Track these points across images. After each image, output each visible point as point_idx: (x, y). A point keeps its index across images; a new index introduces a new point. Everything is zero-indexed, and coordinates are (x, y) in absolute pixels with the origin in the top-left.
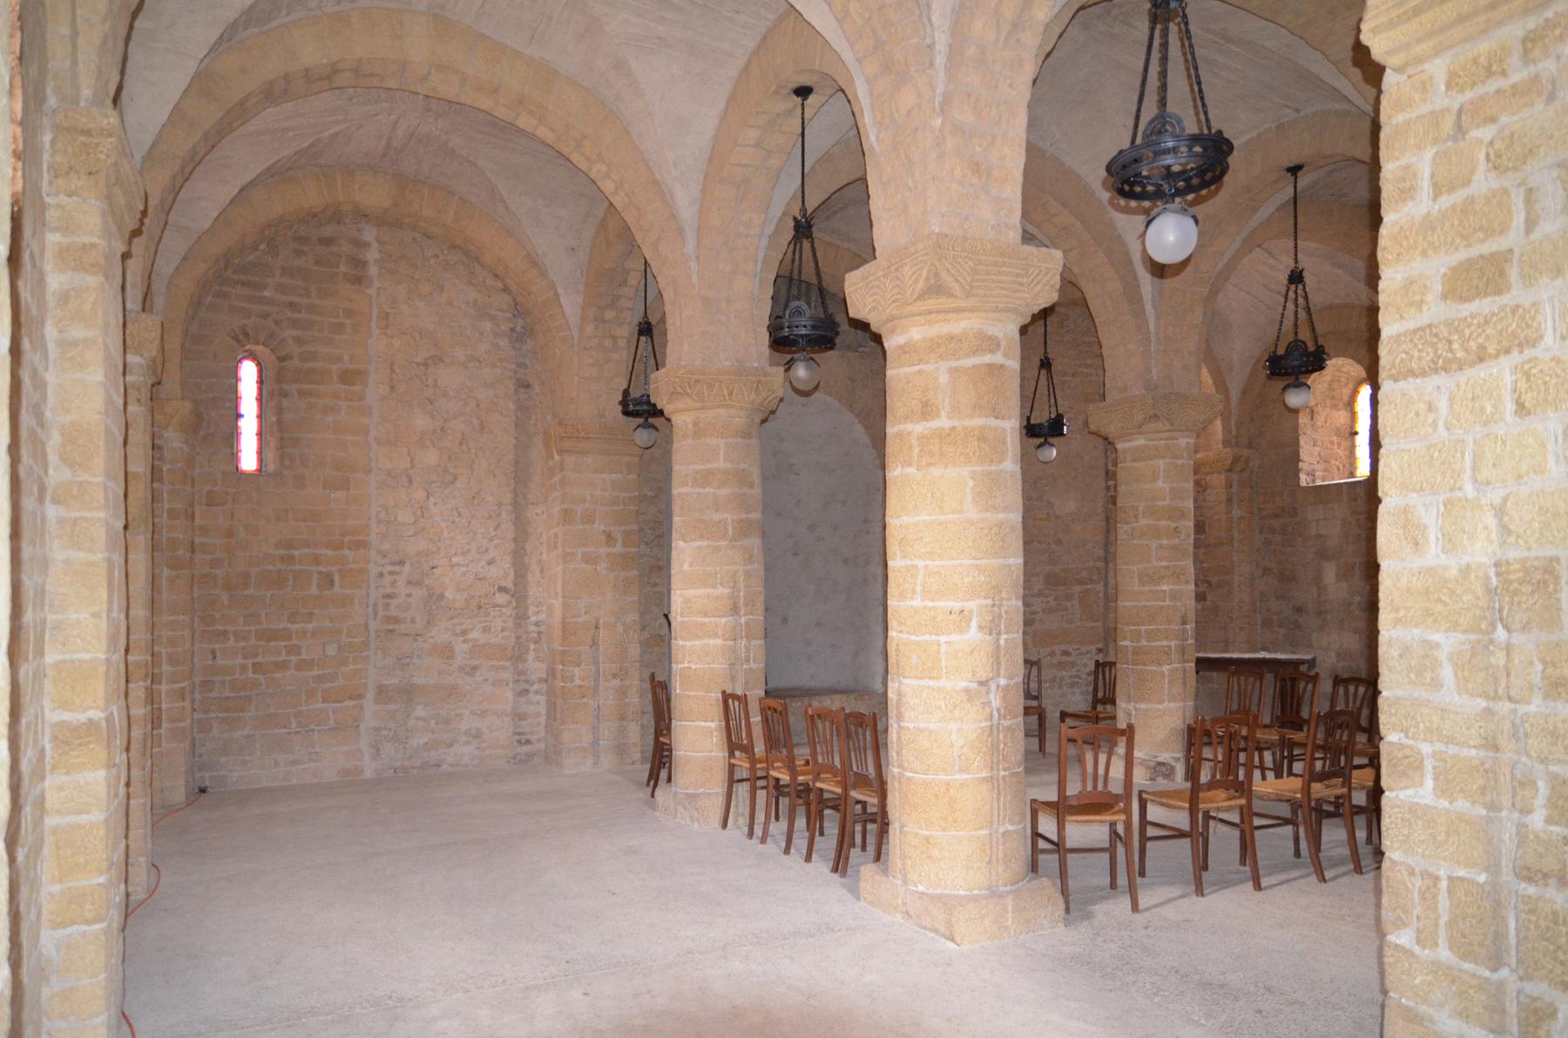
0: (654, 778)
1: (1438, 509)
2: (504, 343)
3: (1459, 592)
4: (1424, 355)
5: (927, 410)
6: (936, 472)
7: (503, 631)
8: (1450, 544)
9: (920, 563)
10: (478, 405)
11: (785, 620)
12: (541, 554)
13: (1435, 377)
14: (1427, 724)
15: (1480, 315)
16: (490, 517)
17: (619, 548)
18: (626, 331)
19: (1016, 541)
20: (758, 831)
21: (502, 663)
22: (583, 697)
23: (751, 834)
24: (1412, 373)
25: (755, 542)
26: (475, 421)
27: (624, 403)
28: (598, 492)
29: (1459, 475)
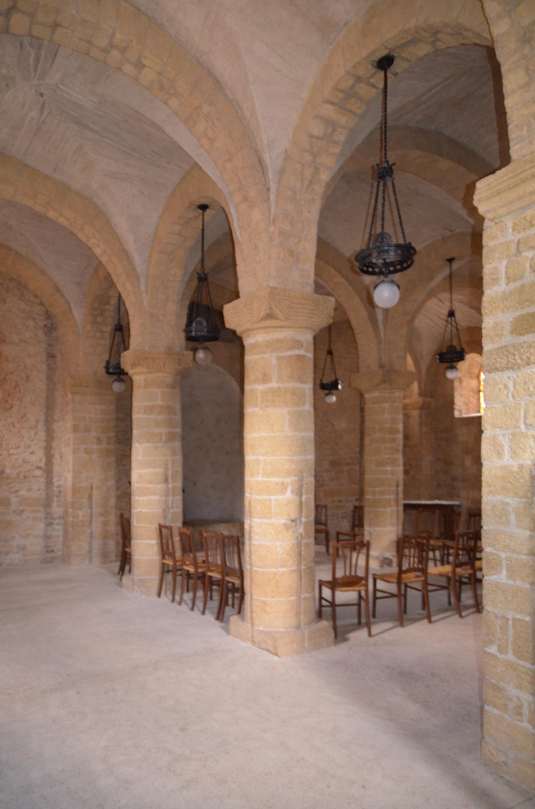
0: (122, 570)
1: (509, 437)
2: (40, 333)
3: (518, 478)
4: (503, 360)
5: (265, 379)
6: (270, 410)
8: (514, 454)
9: (262, 458)
10: (25, 367)
12: (61, 448)
13: (507, 371)
14: (504, 543)
15: (528, 342)
16: (32, 428)
17: (104, 446)
18: (108, 329)
19: (311, 448)
20: (177, 598)
22: (83, 526)
23: (173, 600)
24: (497, 369)
25: (178, 444)
26: (24, 376)
27: (107, 368)
29: (518, 420)
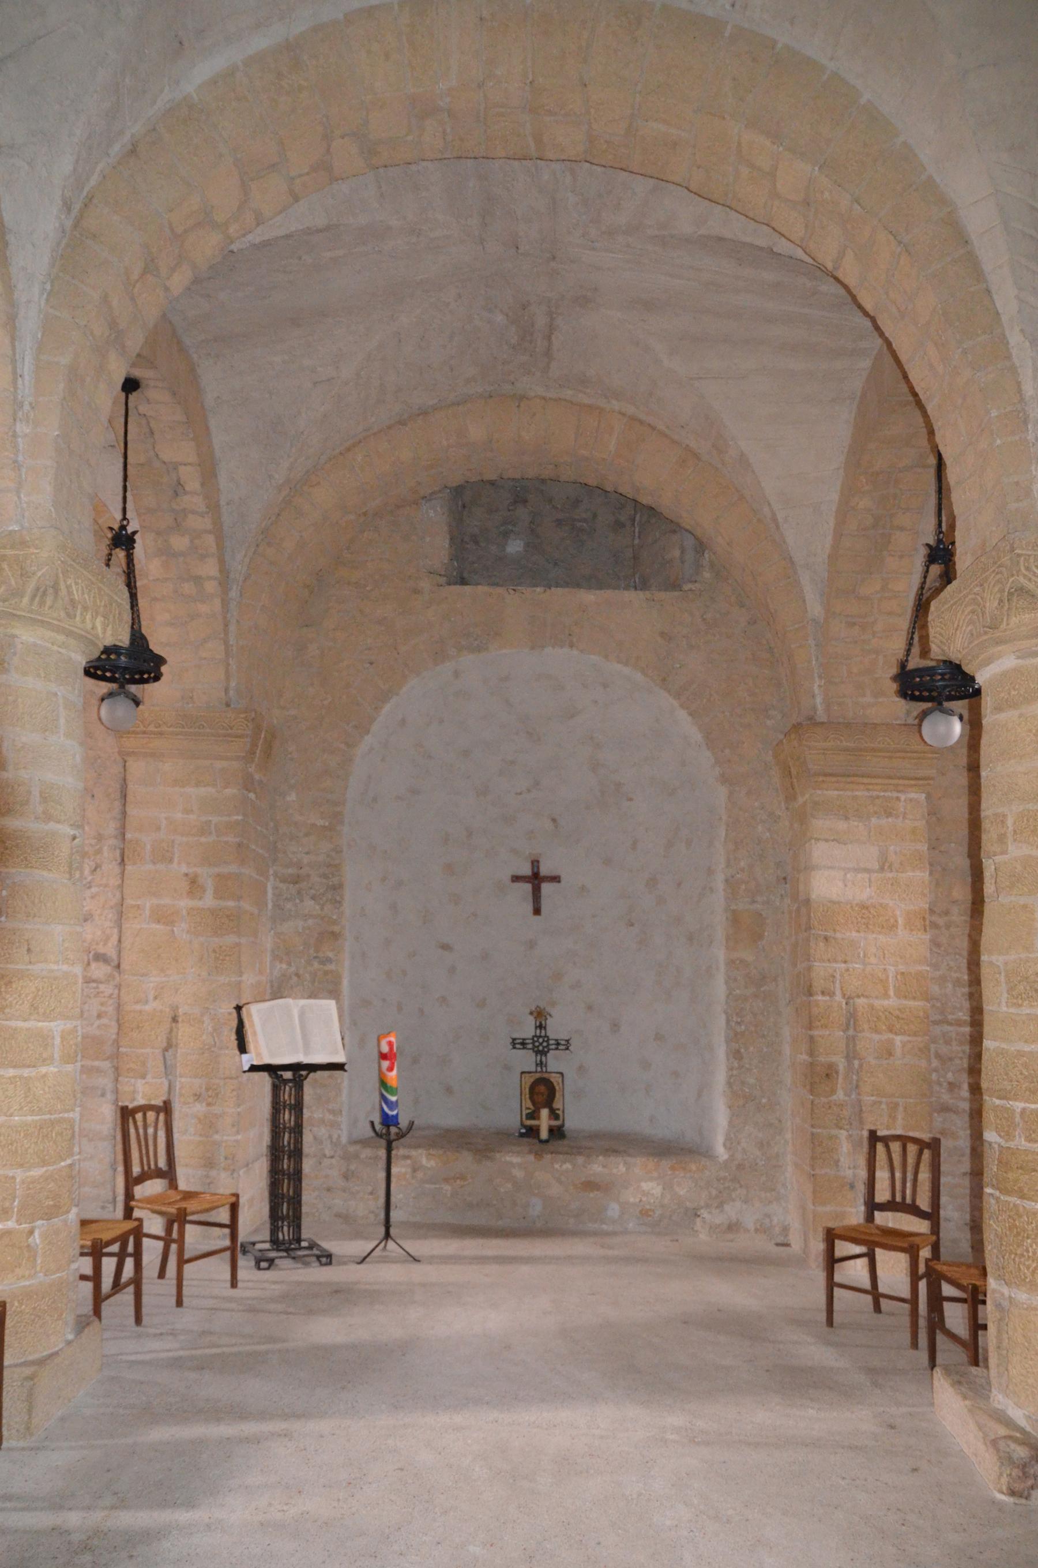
7: (99, 1016)
11: (615, 1027)
21: (96, 1063)
28: (179, 816)
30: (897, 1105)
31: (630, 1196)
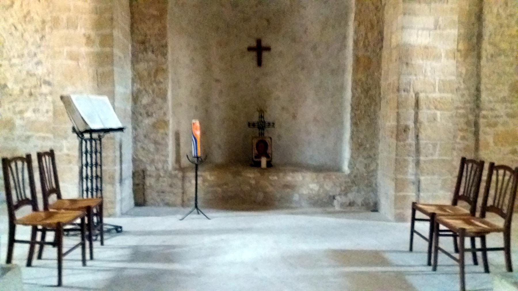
16: (37, 31)
30: (437, 144)
31: (304, 191)
